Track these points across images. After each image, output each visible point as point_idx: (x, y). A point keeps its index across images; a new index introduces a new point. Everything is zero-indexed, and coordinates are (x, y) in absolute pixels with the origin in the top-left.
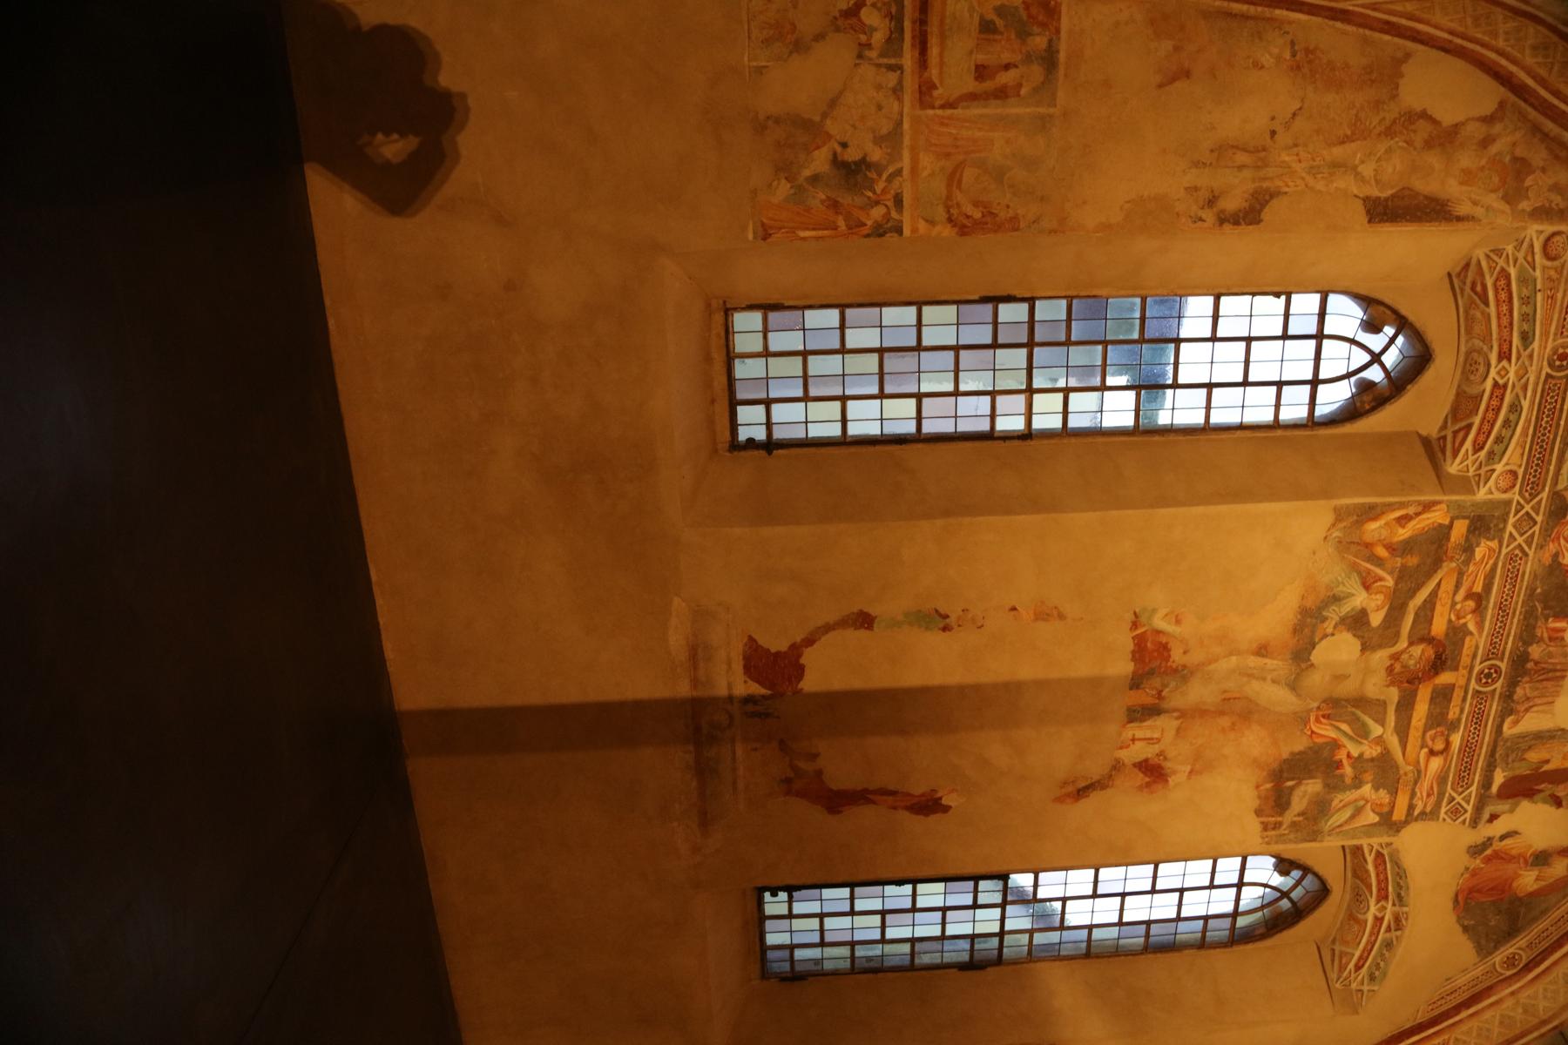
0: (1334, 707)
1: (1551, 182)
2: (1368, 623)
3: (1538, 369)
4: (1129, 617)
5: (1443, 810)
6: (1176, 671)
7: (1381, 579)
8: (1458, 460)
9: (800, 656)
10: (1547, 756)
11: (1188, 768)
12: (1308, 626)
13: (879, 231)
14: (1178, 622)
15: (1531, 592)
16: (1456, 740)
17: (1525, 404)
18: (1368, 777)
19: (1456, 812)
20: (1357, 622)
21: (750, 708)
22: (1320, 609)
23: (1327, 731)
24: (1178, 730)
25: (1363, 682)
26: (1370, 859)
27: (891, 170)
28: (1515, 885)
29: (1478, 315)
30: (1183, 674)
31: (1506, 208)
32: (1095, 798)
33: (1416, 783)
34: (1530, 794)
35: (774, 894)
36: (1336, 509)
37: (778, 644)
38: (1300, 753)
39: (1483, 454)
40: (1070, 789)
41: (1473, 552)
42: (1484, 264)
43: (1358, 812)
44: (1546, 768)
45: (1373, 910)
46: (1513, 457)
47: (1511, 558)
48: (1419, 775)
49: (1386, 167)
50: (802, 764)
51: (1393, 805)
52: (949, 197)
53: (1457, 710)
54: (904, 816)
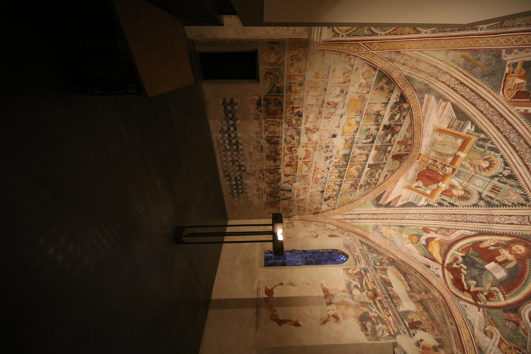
0: (363, 304)
3: (359, 251)
12: (348, 285)
16: (390, 312)
18: (379, 322)
19: (404, 332)
20: (356, 287)
23: (365, 309)
30: (333, 296)
32: (328, 324)
34: (417, 328)
37: (270, 288)
40: (322, 321)
44: (414, 320)
46: (363, 262)
48: (389, 321)
50: (274, 313)
51: (389, 329)
54: (292, 326)
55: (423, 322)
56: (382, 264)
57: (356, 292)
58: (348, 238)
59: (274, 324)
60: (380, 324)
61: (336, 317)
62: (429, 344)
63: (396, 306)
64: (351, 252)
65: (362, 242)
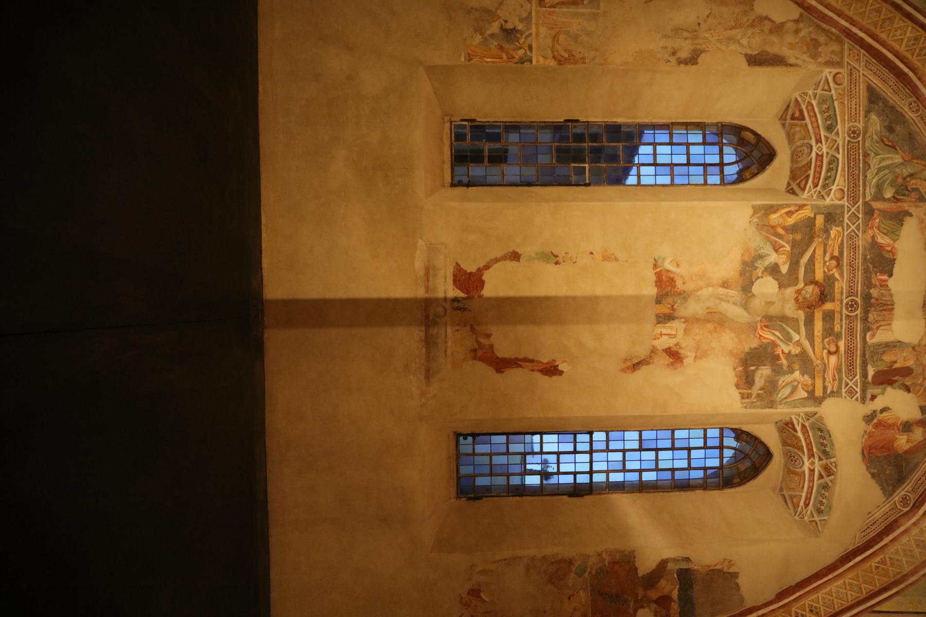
0: (772, 321)
1: (831, 49)
2: (780, 271)
3: (842, 139)
4: (652, 261)
5: (844, 391)
6: (680, 294)
7: (783, 246)
9: (482, 275)
10: (895, 359)
11: (694, 355)
12: (748, 270)
13: (521, 61)
14: (678, 265)
15: (865, 256)
16: (842, 344)
17: (840, 157)
18: (796, 366)
19: (851, 393)
20: (774, 270)
21: (456, 304)
22: (753, 262)
23: (768, 335)
24: (685, 330)
25: (783, 306)
26: (799, 428)
27: (527, 33)
28: (895, 445)
30: (684, 296)
31: (812, 61)
33: (824, 372)
34: (891, 383)
35: (465, 439)
36: (754, 207)
37: (471, 268)
38: (755, 349)
39: (818, 188)
42: (799, 99)
43: (794, 389)
44: (896, 366)
45: (807, 464)
46: (840, 182)
47: (850, 237)
48: (825, 367)
49: (753, 42)
50: (482, 340)
51: (814, 385)
52: (553, 47)
53: (839, 326)
54: (538, 376)
55: (917, 371)
56: (902, 191)
58: (828, 73)
59: (482, 369)
60: (797, 374)
61: (674, 356)
62: (899, 418)
64: (790, 138)
65: (873, 96)
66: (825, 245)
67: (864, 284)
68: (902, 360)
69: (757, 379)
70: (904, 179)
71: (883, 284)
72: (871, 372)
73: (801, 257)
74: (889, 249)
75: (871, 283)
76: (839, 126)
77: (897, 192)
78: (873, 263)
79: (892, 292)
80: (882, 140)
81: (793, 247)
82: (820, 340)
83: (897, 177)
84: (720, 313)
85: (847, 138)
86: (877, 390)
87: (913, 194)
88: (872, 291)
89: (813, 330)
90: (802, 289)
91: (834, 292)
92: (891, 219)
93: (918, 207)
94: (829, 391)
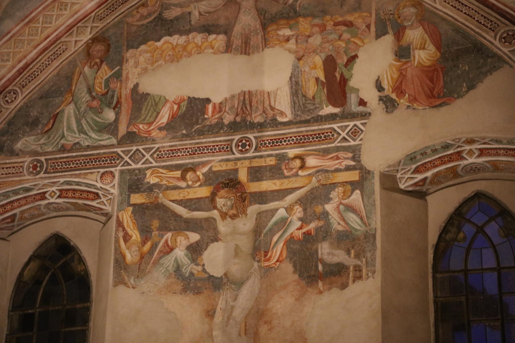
0: (259, 249)
2: (197, 243)
5: (352, 143)
7: (166, 241)
8: (103, 207)
10: (313, 81)
16: (292, 152)
17: (62, 180)
18: (319, 209)
19: (355, 133)
20: (195, 251)
22: (183, 280)
23: (278, 250)
25: (241, 234)
26: (420, 177)
28: (428, 63)
29: (26, 215)
33: (327, 171)
34: (344, 81)
36: (116, 285)
38: (295, 266)
41: (154, 185)
43: (350, 208)
44: (322, 78)
45: (471, 160)
46: (92, 179)
56: (108, 99)
57: (216, 259)
60: (329, 207)
62: (391, 65)
63: (275, 123)
64: (38, 217)
66: (168, 188)
67: (217, 134)
68: (314, 70)
69: (335, 260)
70: (93, 98)
71: (220, 108)
72: (329, 110)
73: (180, 217)
74: (176, 107)
75: (217, 124)
76: (27, 185)
77: (109, 105)
78: (192, 125)
79: (228, 96)
80: (47, 131)
81: (168, 230)
82: (286, 181)
83: (91, 108)
84: (246, 317)
85: (42, 175)
86: (353, 99)
87: (111, 86)
88: (226, 122)
89: (272, 192)
90: (220, 212)
91: (225, 171)
92: (140, 110)
93: (127, 77)
94: (352, 163)
